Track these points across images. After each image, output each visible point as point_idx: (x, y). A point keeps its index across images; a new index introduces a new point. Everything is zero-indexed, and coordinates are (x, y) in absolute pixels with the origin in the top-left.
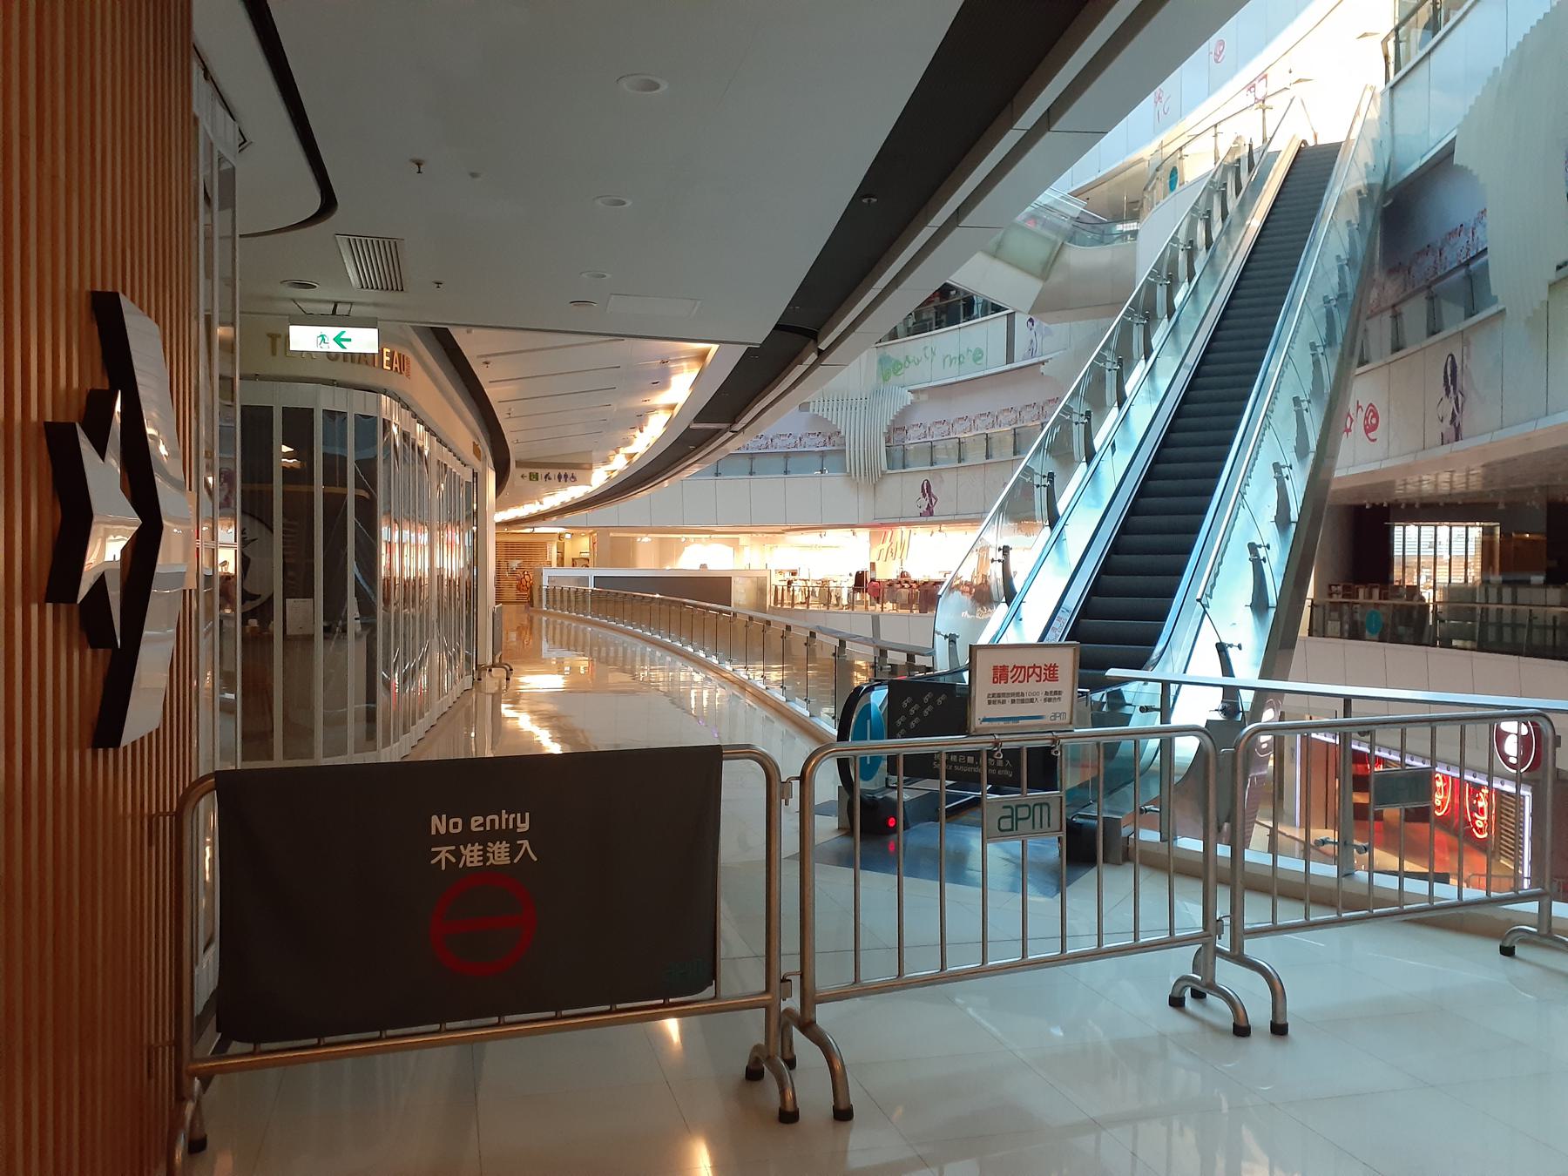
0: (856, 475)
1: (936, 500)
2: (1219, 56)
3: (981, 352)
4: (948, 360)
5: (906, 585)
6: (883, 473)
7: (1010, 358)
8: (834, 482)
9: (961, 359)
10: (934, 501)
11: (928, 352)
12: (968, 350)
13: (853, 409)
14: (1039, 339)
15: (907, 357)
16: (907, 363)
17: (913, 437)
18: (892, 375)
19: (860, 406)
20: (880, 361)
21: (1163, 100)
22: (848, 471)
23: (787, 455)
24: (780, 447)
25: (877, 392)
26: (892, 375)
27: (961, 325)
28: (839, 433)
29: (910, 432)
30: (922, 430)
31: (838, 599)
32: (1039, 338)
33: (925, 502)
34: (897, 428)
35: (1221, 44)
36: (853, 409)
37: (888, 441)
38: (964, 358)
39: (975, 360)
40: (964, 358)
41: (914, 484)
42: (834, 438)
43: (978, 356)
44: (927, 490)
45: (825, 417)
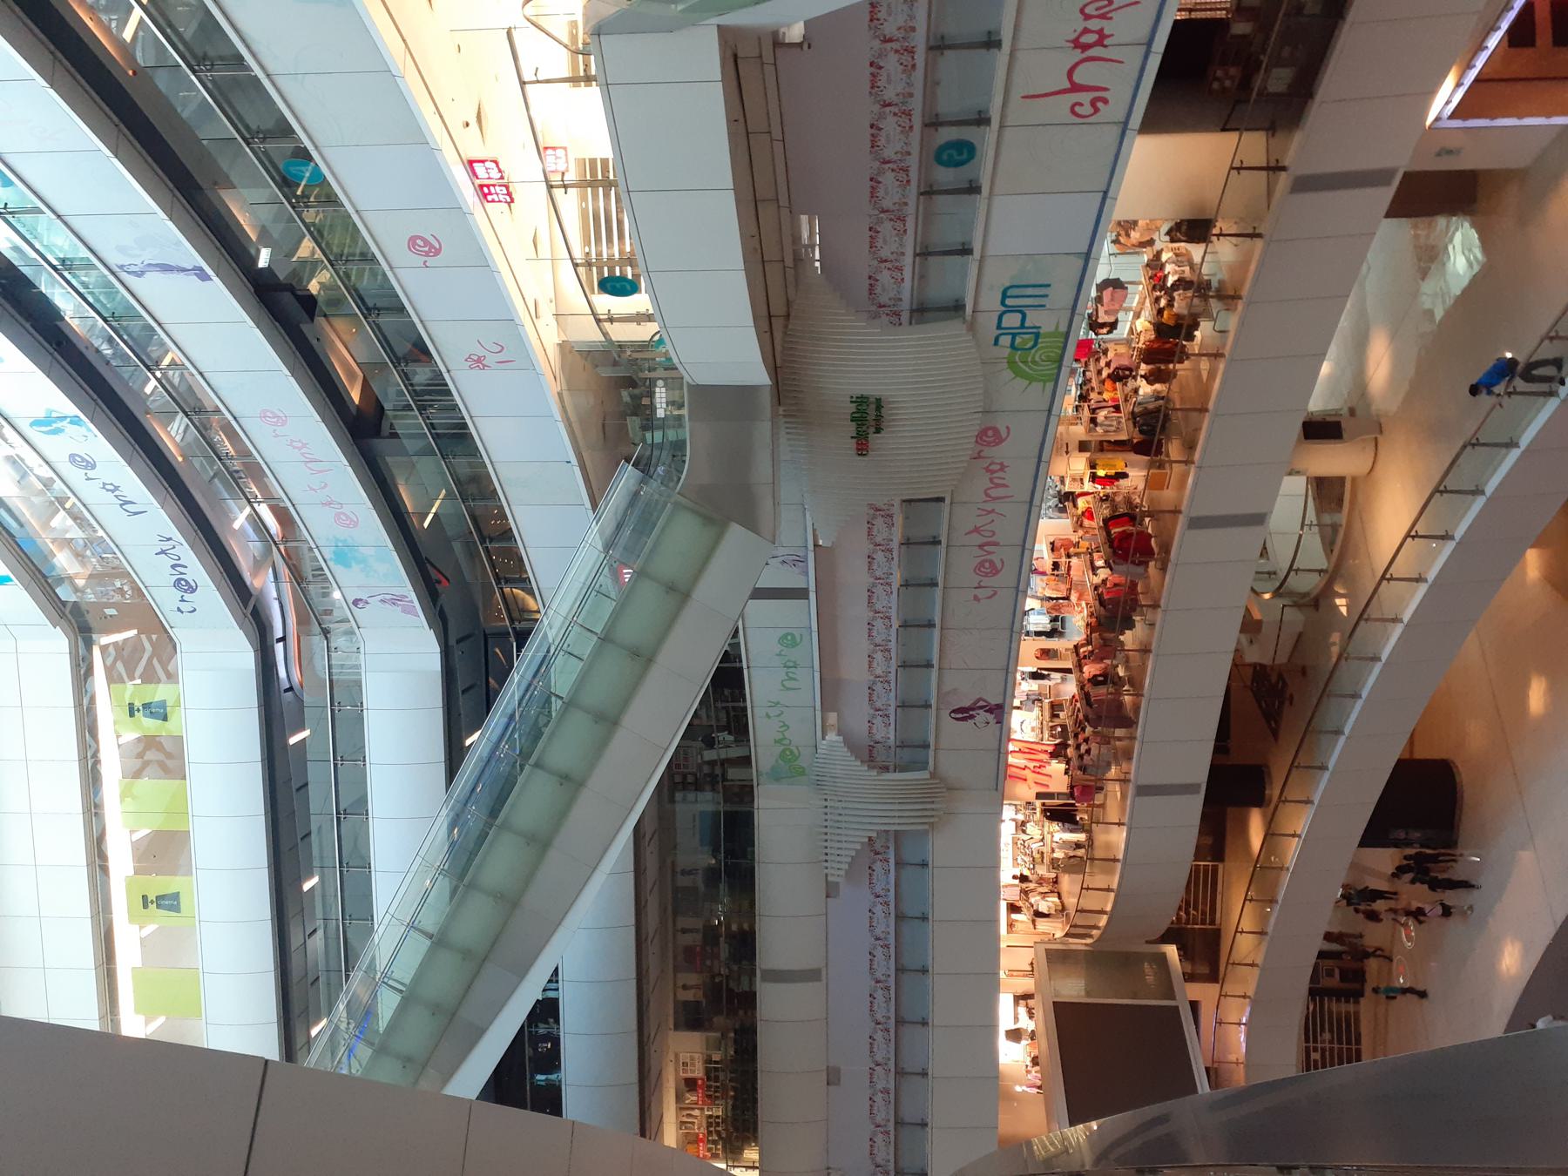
0: (932, 816)
2: (432, 246)
3: (788, 634)
5: (1083, 748)
6: (933, 775)
8: (942, 849)
9: (791, 664)
11: (772, 712)
12: (779, 655)
13: (840, 818)
14: (781, 551)
15: (776, 742)
16: (785, 742)
17: (886, 733)
19: (838, 808)
20: (778, 780)
21: (481, 352)
22: (926, 827)
23: (900, 917)
24: (888, 926)
25: (818, 784)
27: (745, 666)
28: (870, 839)
29: (878, 737)
30: (878, 721)
31: (1078, 845)
32: (781, 551)
33: (982, 716)
34: (870, 755)
35: (415, 244)
36: (840, 818)
37: (886, 769)
38: (789, 661)
39: (794, 644)
40: (789, 661)
41: (954, 731)
42: (878, 846)
43: (789, 641)
44: (964, 713)
45: (849, 860)
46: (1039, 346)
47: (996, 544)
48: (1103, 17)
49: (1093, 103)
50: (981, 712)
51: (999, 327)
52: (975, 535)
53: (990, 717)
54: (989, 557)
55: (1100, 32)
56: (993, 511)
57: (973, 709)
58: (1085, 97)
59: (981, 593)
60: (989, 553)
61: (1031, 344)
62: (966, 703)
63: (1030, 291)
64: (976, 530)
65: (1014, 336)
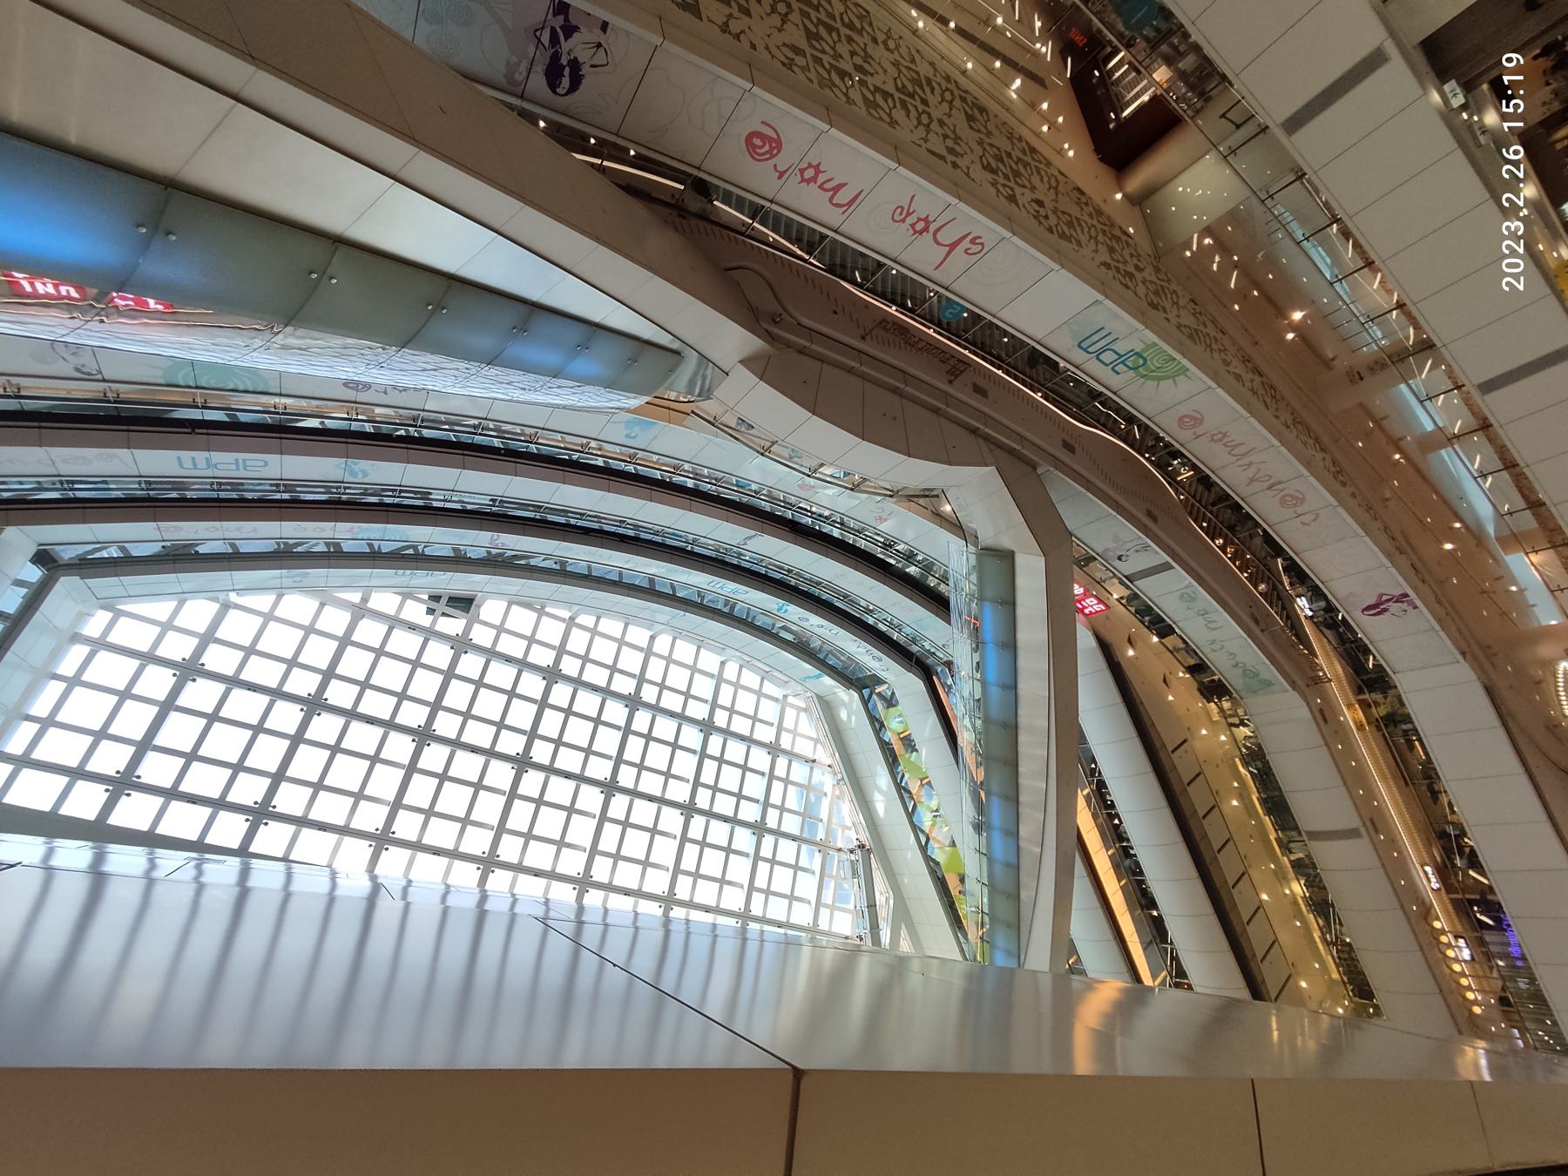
1: (1381, 595)
3: (1182, 596)
4: (1212, 625)
7: (1166, 567)
10: (1385, 598)
11: (1215, 646)
18: (1260, 677)
26: (1260, 677)
33: (1394, 607)
44: (1377, 608)
46: (1148, 358)
47: (1280, 483)
48: (908, 214)
49: (973, 241)
50: (1389, 604)
51: (1106, 365)
52: (1255, 484)
53: (1405, 606)
54: (1283, 493)
55: (919, 219)
56: (1250, 464)
57: (1382, 604)
58: (965, 244)
59: (1305, 519)
60: (1281, 490)
61: (1141, 362)
62: (1372, 601)
63: (1095, 338)
64: (1252, 480)
65: (1122, 362)
